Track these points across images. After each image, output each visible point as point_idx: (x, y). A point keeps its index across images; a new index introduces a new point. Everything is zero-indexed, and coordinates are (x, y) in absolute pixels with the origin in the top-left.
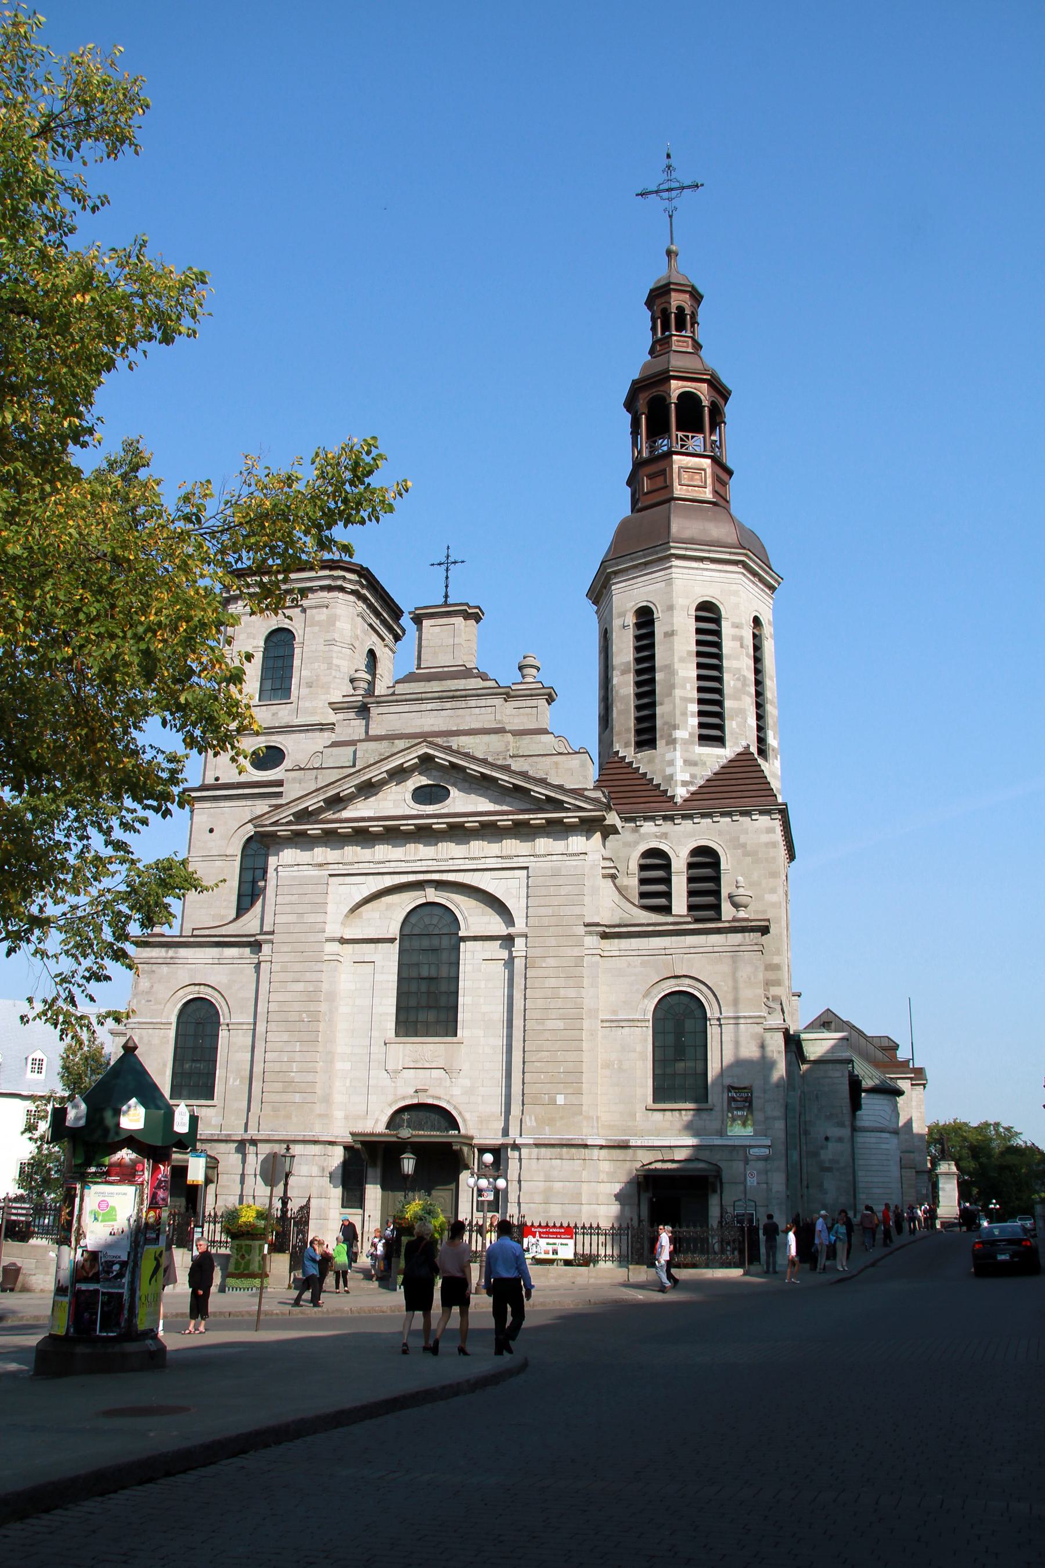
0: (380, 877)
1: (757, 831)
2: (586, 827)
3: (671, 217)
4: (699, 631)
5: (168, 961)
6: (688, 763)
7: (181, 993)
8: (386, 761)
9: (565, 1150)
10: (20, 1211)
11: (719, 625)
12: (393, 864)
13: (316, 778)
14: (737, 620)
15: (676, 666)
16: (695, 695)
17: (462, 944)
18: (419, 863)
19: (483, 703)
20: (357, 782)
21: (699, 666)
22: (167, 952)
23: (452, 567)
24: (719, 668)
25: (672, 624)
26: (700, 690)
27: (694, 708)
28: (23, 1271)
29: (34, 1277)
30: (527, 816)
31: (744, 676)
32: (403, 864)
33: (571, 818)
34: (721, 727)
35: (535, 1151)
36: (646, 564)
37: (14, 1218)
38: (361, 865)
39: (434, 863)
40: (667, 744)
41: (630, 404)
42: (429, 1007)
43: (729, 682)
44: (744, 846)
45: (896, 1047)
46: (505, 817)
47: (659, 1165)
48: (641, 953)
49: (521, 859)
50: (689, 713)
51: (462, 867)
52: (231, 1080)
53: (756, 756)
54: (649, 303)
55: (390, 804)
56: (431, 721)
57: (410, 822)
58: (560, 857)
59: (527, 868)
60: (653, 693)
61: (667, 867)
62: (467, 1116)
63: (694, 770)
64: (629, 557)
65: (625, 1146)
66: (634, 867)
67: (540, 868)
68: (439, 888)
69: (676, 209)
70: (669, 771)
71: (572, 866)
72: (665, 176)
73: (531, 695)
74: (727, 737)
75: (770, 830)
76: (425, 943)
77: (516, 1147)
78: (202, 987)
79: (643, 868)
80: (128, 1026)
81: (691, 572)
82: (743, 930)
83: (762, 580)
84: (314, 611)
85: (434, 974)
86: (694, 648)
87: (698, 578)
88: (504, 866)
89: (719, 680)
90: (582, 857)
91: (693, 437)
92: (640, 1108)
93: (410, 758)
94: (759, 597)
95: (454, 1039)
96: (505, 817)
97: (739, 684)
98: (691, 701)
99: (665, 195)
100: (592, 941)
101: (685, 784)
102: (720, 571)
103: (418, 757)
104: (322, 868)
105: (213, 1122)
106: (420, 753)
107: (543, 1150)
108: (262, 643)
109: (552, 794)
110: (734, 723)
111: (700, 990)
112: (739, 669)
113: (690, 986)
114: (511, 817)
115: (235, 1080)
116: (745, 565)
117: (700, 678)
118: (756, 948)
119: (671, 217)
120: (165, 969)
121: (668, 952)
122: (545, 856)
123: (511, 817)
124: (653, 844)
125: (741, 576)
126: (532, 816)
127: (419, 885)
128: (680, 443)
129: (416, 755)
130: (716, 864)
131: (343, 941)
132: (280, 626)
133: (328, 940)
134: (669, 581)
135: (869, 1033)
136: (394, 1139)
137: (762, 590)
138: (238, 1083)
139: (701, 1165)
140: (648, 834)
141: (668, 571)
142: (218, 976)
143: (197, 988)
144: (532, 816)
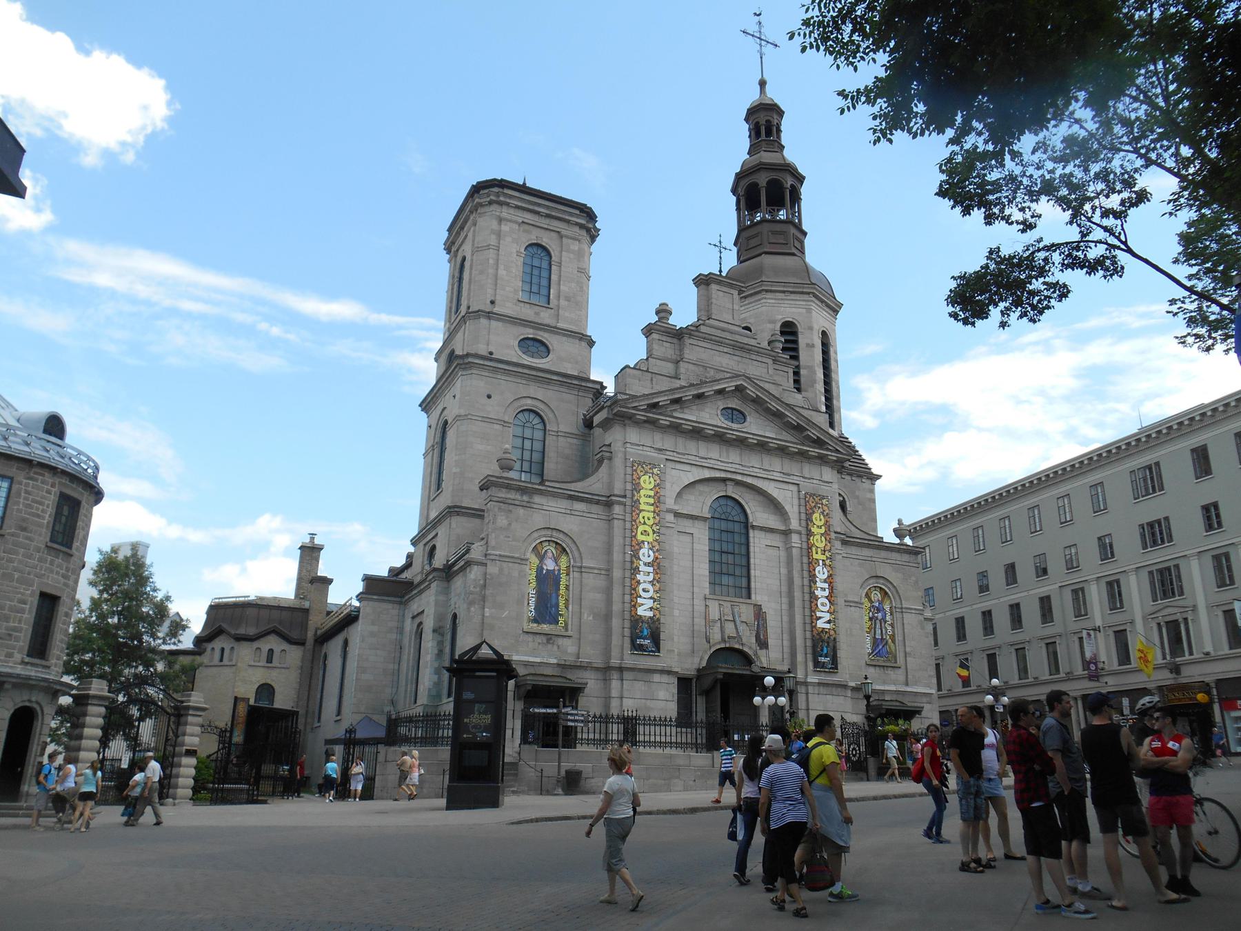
0: (700, 470)
3: (761, 58)
5: (524, 504)
7: (536, 535)
9: (834, 689)
10: (577, 718)
12: (712, 462)
13: (652, 380)
15: (817, 368)
18: (730, 465)
19: (760, 359)
20: (695, 392)
25: (812, 340)
28: (584, 775)
29: (593, 781)
32: (719, 463)
33: (833, 456)
35: (817, 688)
36: (792, 292)
37: (570, 724)
38: (690, 457)
44: (857, 497)
46: (795, 446)
48: (858, 557)
49: (795, 478)
51: (759, 475)
52: (586, 615)
55: (708, 416)
58: (817, 482)
59: (798, 484)
76: (724, 525)
77: (806, 684)
80: (488, 557)
84: (570, 241)
85: (730, 550)
90: (830, 485)
93: (730, 385)
96: (795, 446)
105: (569, 651)
106: (739, 383)
107: (822, 690)
108: (522, 250)
109: (822, 438)
111: (889, 588)
113: (883, 584)
114: (799, 447)
115: (589, 616)
119: (761, 58)
120: (521, 511)
121: (874, 559)
122: (809, 479)
123: (799, 447)
127: (724, 480)
129: (735, 384)
131: (677, 515)
132: (539, 242)
133: (669, 511)
134: (809, 311)
136: (748, 673)
138: (591, 618)
141: (810, 303)
142: (570, 525)
143: (549, 532)
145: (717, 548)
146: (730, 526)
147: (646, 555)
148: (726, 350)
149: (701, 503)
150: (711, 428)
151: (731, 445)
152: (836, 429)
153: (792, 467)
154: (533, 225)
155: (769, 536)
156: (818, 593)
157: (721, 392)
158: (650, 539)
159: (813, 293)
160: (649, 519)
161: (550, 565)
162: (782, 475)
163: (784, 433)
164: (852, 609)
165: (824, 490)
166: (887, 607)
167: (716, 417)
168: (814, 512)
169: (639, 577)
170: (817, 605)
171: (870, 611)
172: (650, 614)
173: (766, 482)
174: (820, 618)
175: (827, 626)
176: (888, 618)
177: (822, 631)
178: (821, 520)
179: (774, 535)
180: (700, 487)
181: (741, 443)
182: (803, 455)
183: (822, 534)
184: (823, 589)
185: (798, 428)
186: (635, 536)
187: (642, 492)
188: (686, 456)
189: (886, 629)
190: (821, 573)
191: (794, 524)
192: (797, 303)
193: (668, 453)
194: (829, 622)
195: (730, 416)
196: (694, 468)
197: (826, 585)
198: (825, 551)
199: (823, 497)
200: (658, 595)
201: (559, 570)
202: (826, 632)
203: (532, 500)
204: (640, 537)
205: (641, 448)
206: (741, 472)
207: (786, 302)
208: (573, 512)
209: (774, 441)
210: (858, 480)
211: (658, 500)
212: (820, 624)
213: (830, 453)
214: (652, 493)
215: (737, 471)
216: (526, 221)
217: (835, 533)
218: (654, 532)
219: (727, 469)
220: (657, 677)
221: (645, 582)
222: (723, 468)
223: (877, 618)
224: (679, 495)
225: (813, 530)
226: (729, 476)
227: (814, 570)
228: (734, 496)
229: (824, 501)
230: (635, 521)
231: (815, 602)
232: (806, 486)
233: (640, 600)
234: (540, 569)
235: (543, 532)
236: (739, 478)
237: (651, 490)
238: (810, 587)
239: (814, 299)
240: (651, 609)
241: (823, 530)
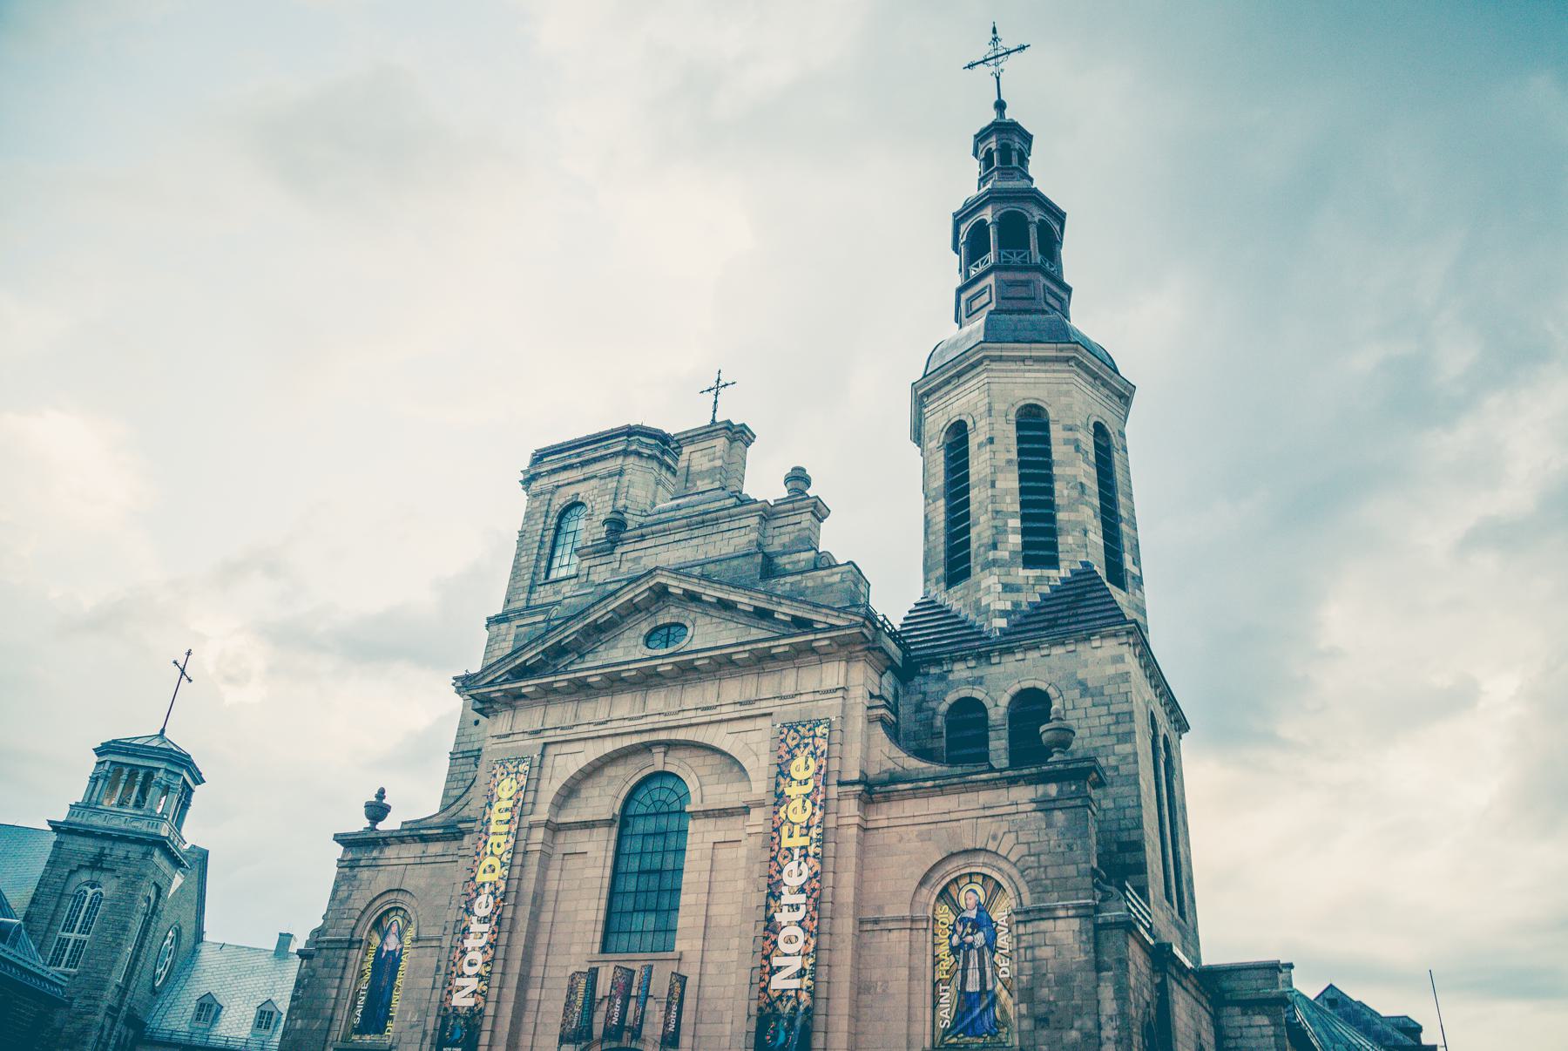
0: (600, 741)
1: (1099, 662)
2: (844, 653)
4: (1020, 440)
6: (1008, 588)
7: (378, 903)
8: (613, 597)
11: (1048, 431)
12: (615, 724)
14: (1069, 422)
16: (1017, 507)
17: (691, 822)
21: (1022, 478)
22: (371, 852)
23: (722, 391)
26: (1023, 504)
27: (1015, 523)
30: (767, 645)
31: (1081, 484)
32: (627, 723)
34: (1054, 546)
36: (959, 375)
38: (580, 729)
39: (662, 718)
42: (645, 911)
43: (1062, 491)
45: (1419, 1029)
48: (916, 820)
49: (764, 704)
50: (1009, 530)
51: (694, 721)
53: (1105, 581)
56: (680, 553)
57: (631, 666)
58: (810, 697)
59: (771, 714)
60: (967, 516)
63: (1015, 597)
64: (939, 371)
67: (786, 713)
68: (670, 753)
71: (826, 707)
73: (794, 510)
75: (1119, 659)
78: (401, 893)
81: (1010, 374)
83: (1105, 384)
86: (1014, 456)
87: (1018, 380)
88: (743, 714)
89: (1051, 492)
90: (840, 693)
91: (1018, 254)
93: (640, 591)
94: (1104, 403)
95: (669, 955)
96: (741, 648)
97: (1075, 494)
98: (1012, 515)
100: (851, 807)
101: (1004, 614)
102: (1046, 371)
103: (650, 588)
104: (539, 736)
106: (651, 584)
109: (799, 614)
110: (1070, 540)
112: (1075, 476)
113: (985, 865)
114: (747, 647)
116: (1079, 364)
117: (1023, 491)
118: (1079, 802)
121: (954, 816)
123: (747, 647)
124: (965, 692)
125: (1072, 375)
126: (772, 643)
127: (647, 747)
128: (1002, 260)
135: (1383, 1015)
137: (1107, 397)
140: (959, 680)
144: (772, 643)
145: (634, 865)
146: (663, 821)
147: (484, 904)
148: (678, 537)
149: (602, 801)
150: (594, 672)
151: (649, 687)
152: (1062, 564)
153: (768, 685)
154: (569, 484)
155: (723, 823)
156: (782, 917)
157: (633, 609)
158: (493, 877)
159: (985, 357)
160: (499, 846)
161: (392, 943)
162: (738, 707)
163: (753, 631)
164: (895, 935)
165: (830, 708)
166: (1000, 915)
167: (633, 650)
168: (793, 757)
169: (469, 943)
170: (775, 943)
171: (955, 931)
172: (471, 1002)
173: (712, 729)
174: (779, 968)
175: (795, 983)
176: (1003, 940)
177: (780, 998)
178: (807, 768)
179: (733, 819)
180: (611, 771)
181: (687, 673)
182: (762, 661)
183: (807, 796)
184: (795, 908)
185: (762, 614)
186: (473, 879)
187: (496, 806)
188: (575, 730)
189: (995, 965)
190: (794, 875)
191: (760, 787)
193: (548, 733)
194: (801, 974)
195: (664, 639)
196: (590, 743)
197: (802, 898)
198: (808, 828)
199: (818, 723)
200: (488, 969)
201: (401, 950)
202: (789, 998)
203: (382, 856)
204: (481, 878)
205: (510, 739)
206: (664, 725)
207: (952, 394)
208: (424, 861)
209: (700, 655)
210: (1081, 647)
211: (522, 808)
212: (778, 983)
213: (811, 637)
214: (510, 804)
215: (657, 726)
216: (560, 483)
217: (840, 784)
218: (503, 864)
219: (638, 728)
221: (474, 949)
222: (633, 729)
223: (971, 946)
224: (570, 791)
225: (788, 791)
226: (646, 738)
227: (780, 872)
228: (669, 768)
229: (820, 730)
230: (478, 854)
231: (773, 937)
232: (790, 711)
233: (459, 982)
234: (380, 950)
235: (386, 898)
236: (663, 736)
237: (511, 798)
238: (768, 907)
239: (994, 366)
240: (474, 992)
241: (809, 788)
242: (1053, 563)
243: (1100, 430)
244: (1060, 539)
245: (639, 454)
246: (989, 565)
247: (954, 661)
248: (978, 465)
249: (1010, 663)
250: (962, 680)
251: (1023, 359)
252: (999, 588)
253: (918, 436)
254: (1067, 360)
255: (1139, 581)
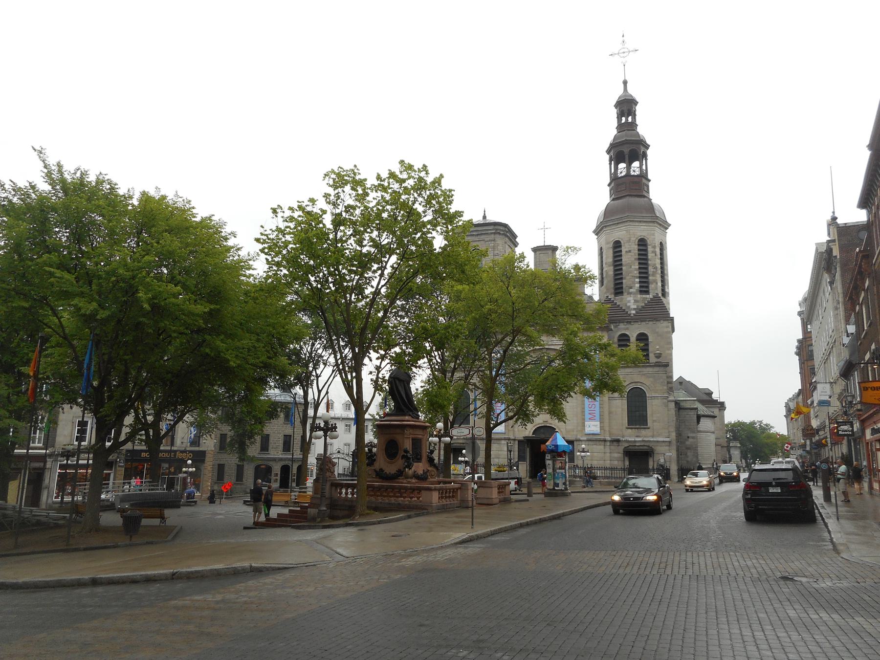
4: (639, 250)
6: (636, 301)
9: (598, 442)
16: (638, 275)
21: (639, 263)
23: (546, 230)
24: (646, 264)
34: (647, 287)
40: (628, 294)
41: (608, 152)
43: (651, 270)
44: (657, 333)
47: (630, 447)
54: (616, 106)
61: (629, 340)
62: (562, 430)
63: (637, 304)
65: (618, 441)
66: (616, 340)
69: (626, 62)
70: (628, 304)
72: (621, 46)
74: (650, 291)
79: (619, 340)
82: (659, 366)
89: (647, 268)
92: (624, 427)
99: (622, 55)
101: (634, 309)
107: (590, 443)
110: (653, 286)
116: (658, 223)
124: (623, 332)
130: (647, 339)
139: (645, 447)
192: (622, 228)
210: (657, 323)
220: (503, 442)
239: (631, 223)
242: (647, 292)
243: (661, 243)
244: (650, 285)
245: (499, 233)
246: (630, 293)
247: (620, 322)
248: (625, 259)
249: (636, 325)
250: (622, 329)
251: (640, 221)
252: (633, 301)
253: (597, 232)
254: (654, 222)
255: (668, 293)
